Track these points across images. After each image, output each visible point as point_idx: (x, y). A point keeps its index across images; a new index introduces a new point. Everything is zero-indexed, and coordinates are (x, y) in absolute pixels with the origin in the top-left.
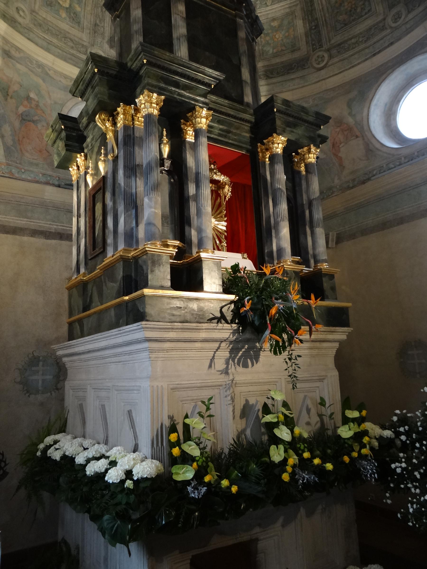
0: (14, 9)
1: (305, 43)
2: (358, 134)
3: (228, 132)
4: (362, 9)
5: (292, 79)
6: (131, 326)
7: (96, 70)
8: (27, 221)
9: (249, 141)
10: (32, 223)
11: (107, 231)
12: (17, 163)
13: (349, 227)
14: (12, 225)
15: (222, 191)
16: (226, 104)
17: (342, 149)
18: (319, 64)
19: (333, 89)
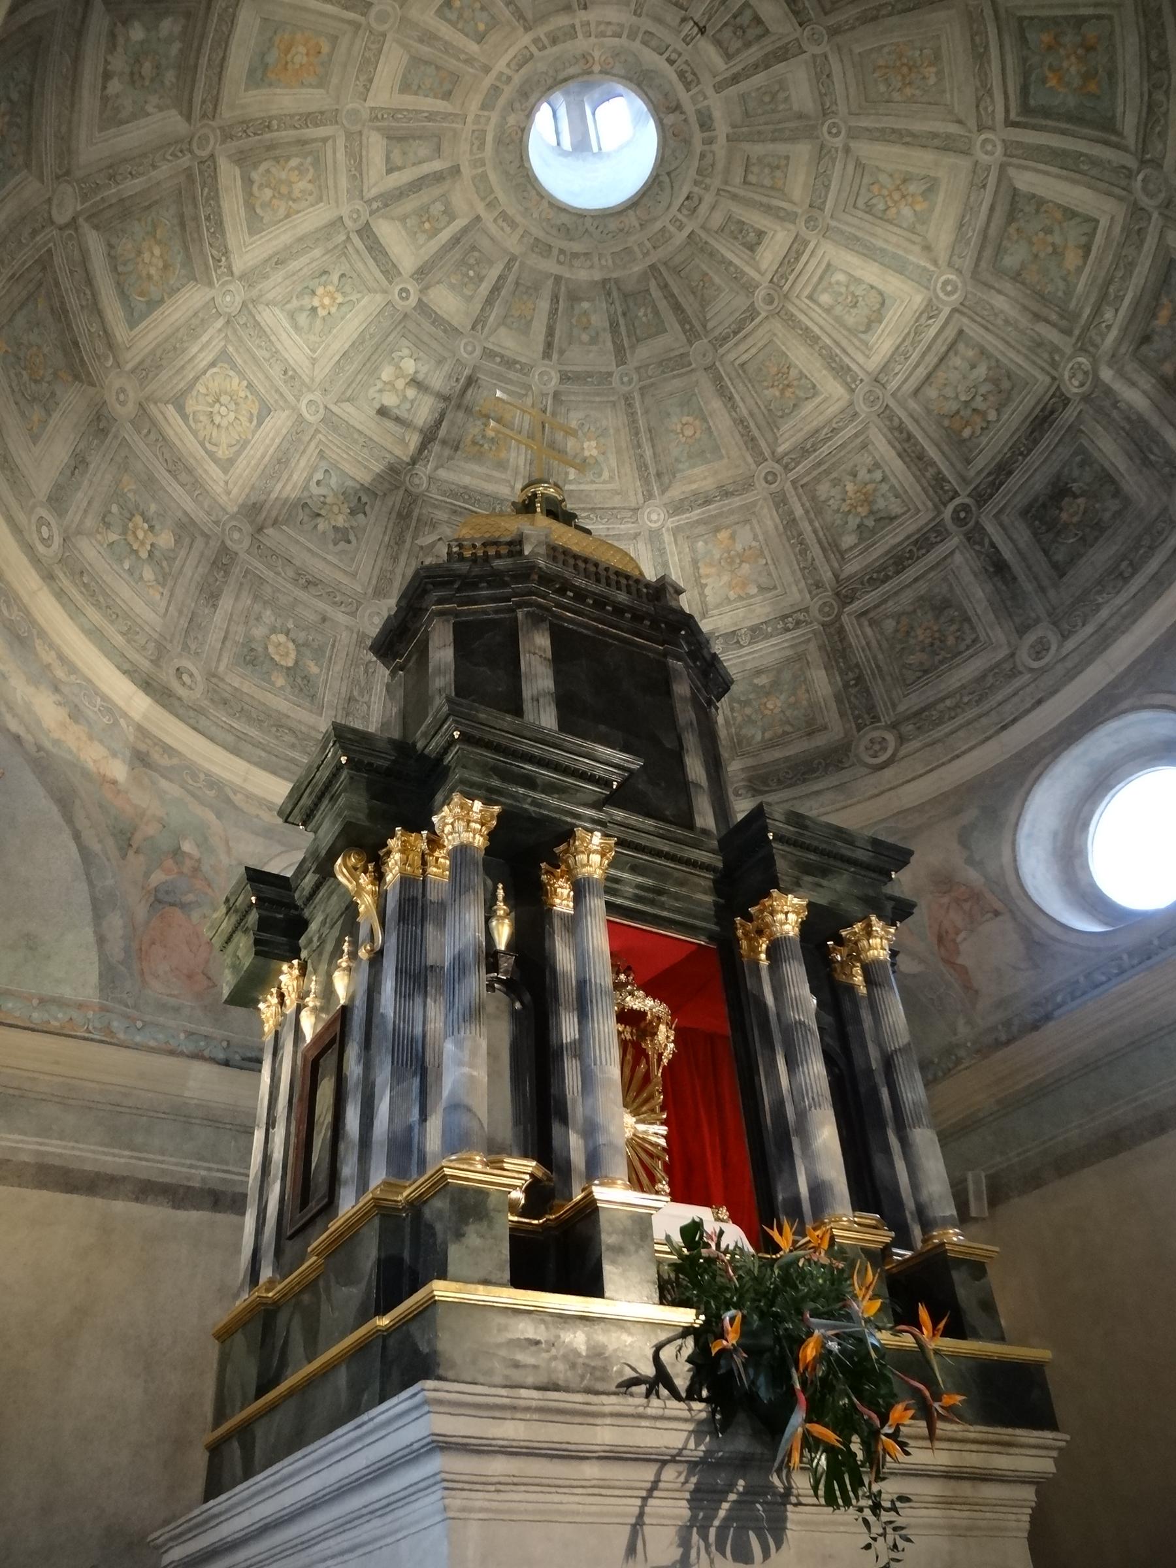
0: (172, 671)
1: (837, 716)
2: (998, 905)
3: (660, 892)
4: (957, 638)
5: (818, 793)
6: (394, 1400)
7: (344, 760)
8: (131, 1157)
9: (712, 913)
10: (144, 1163)
11: (342, 1147)
12: (127, 1006)
13: (1019, 1155)
14: (88, 1167)
15: (652, 1041)
16: (652, 829)
17: (964, 947)
19: (920, 809)
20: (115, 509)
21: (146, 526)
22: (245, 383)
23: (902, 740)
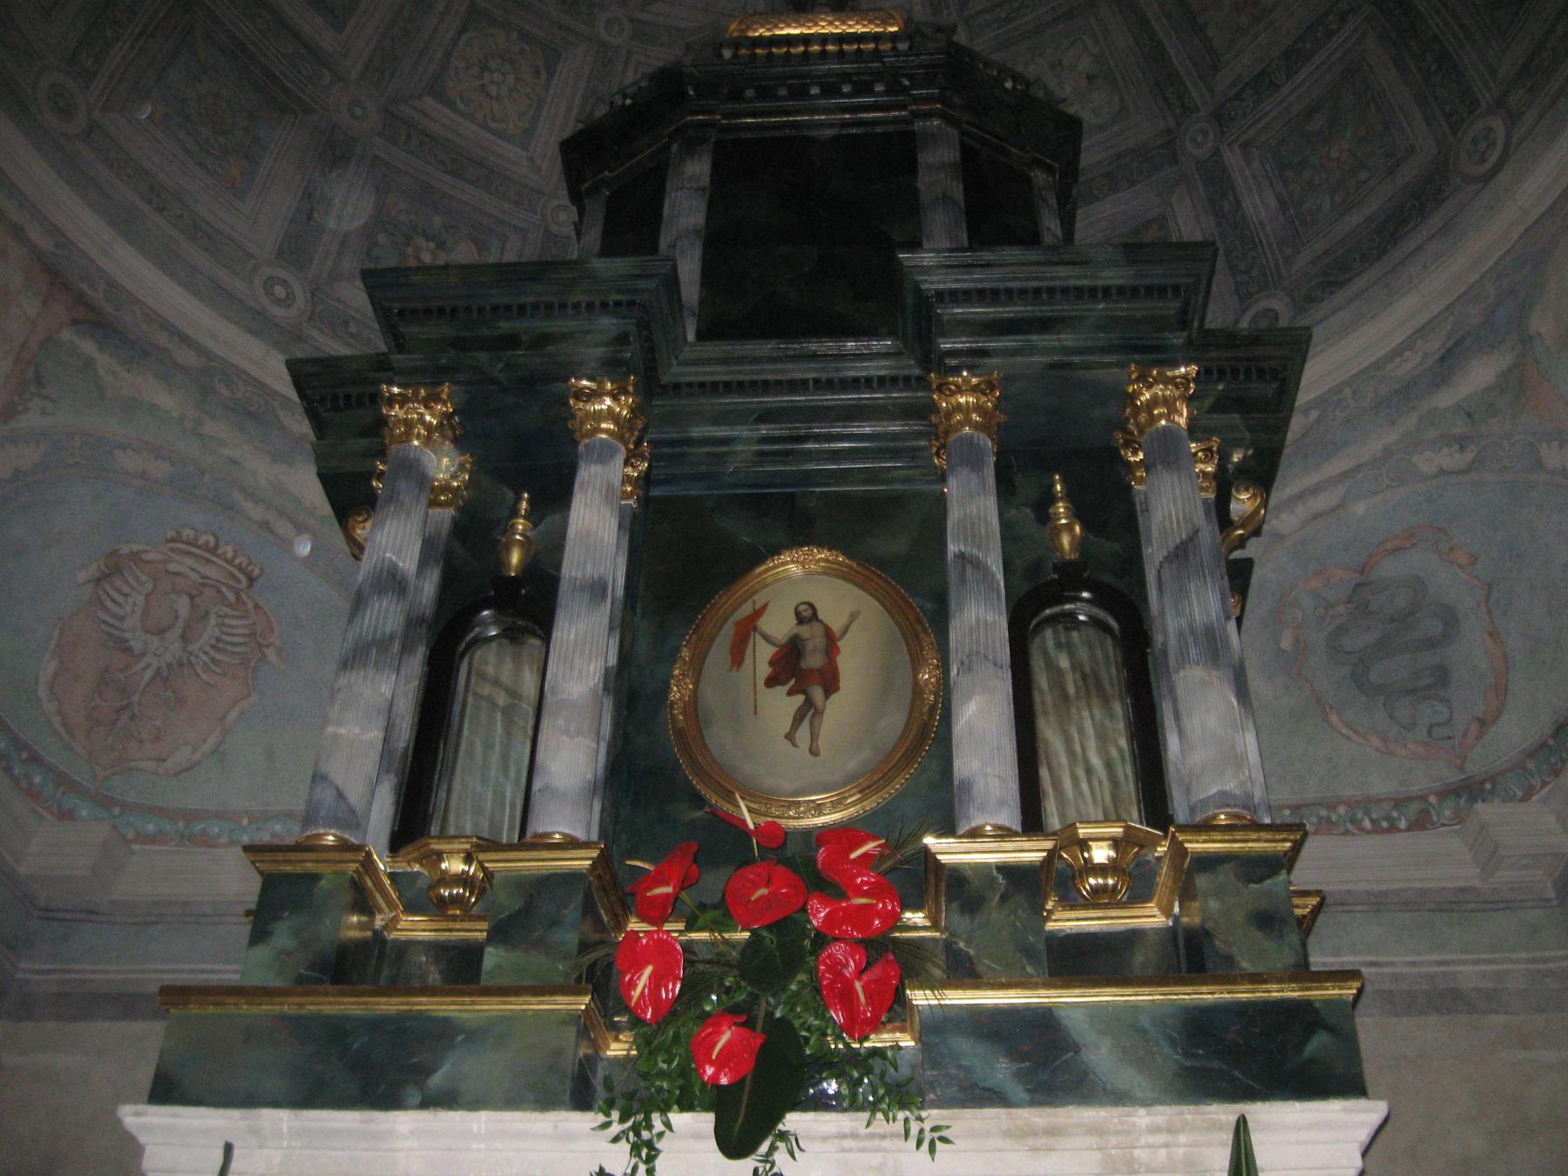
18: (1484, 161)
20: (382, 239)
21: (432, 245)
22: (514, 35)
23: (1513, 118)
